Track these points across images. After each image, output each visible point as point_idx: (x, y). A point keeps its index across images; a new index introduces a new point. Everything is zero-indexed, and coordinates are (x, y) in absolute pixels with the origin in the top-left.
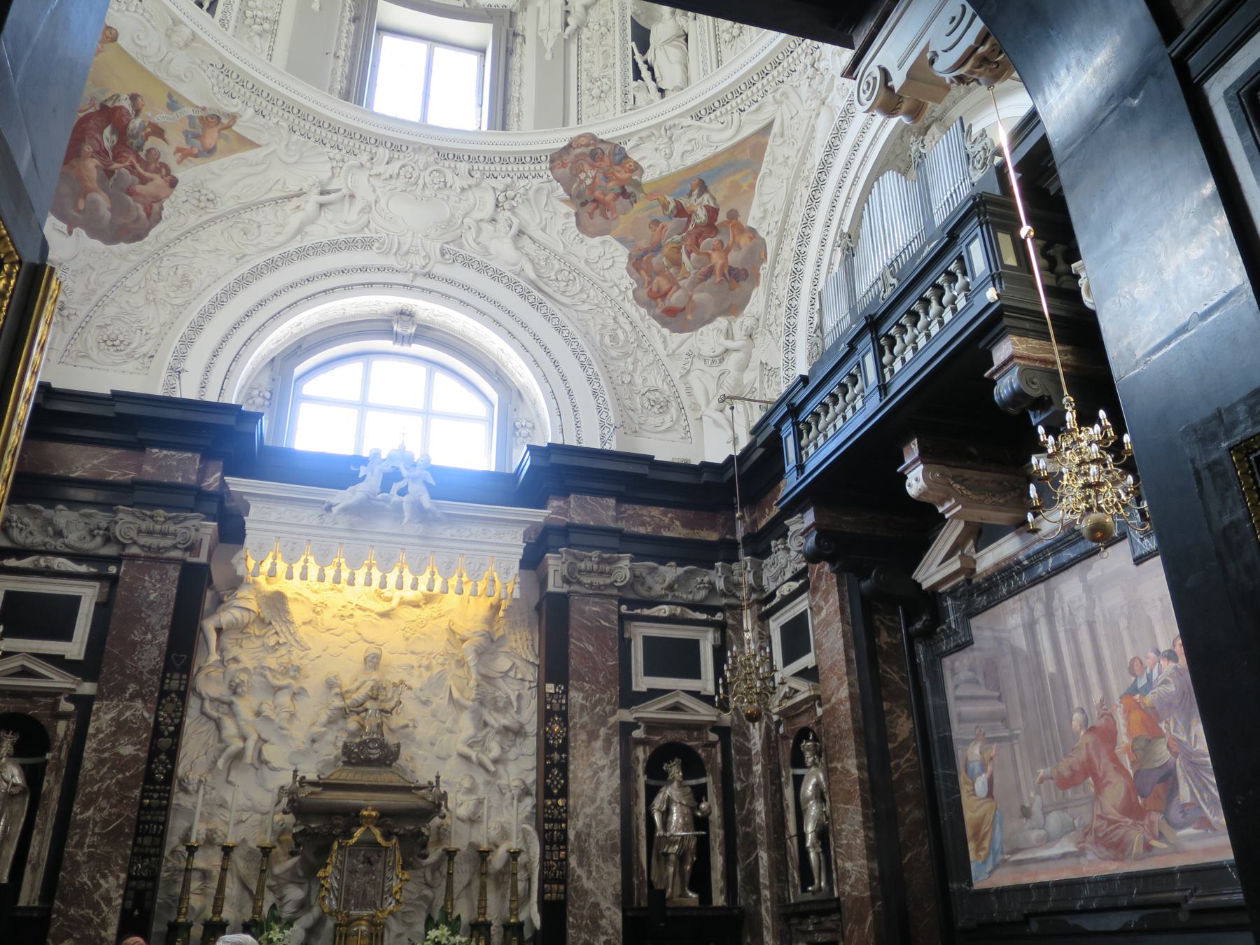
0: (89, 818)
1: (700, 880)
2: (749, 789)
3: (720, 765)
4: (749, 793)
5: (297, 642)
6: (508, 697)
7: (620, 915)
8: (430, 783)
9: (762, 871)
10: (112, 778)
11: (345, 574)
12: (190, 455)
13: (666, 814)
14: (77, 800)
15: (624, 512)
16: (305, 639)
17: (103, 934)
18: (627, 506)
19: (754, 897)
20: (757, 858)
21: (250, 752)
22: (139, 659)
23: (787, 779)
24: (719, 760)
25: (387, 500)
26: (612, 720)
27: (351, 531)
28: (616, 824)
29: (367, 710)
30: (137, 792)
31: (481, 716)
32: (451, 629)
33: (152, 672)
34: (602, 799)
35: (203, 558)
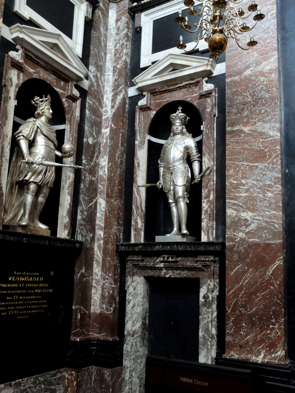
1: (49, 214)
2: (95, 147)
4: (97, 149)
9: (98, 215)
13: (32, 144)
19: (91, 235)
20: (96, 203)
23: (142, 143)
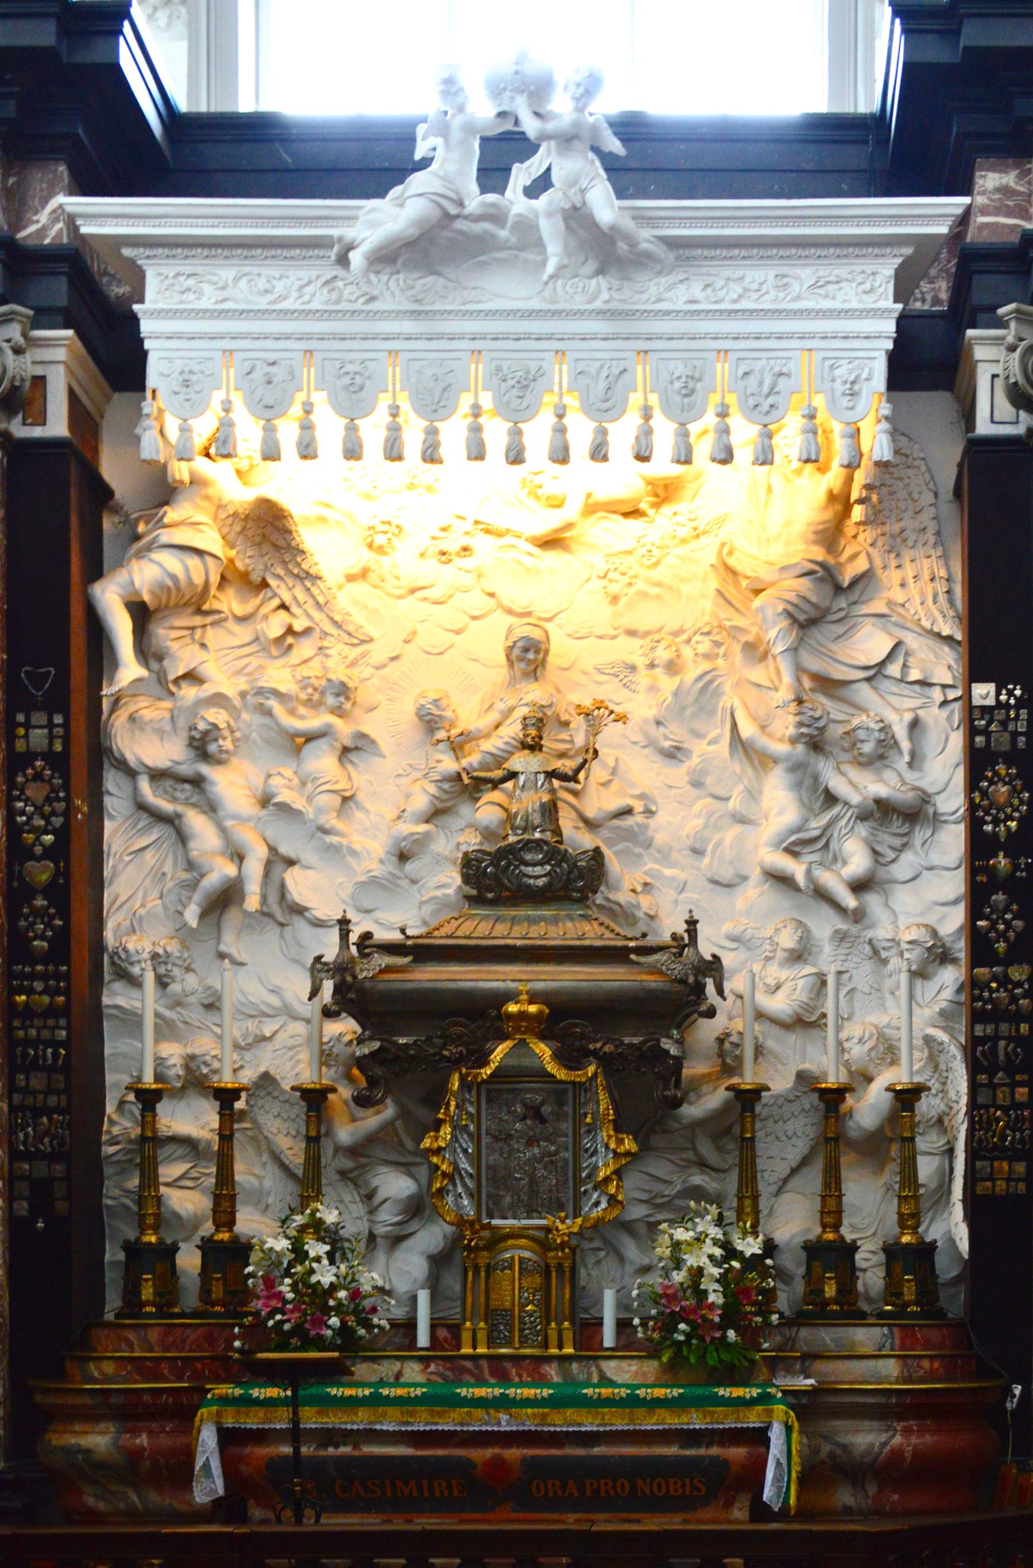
6: (885, 729)
11: (413, 440)
21: (253, 890)
25: (496, 216)
27: (416, 315)
31: (816, 778)
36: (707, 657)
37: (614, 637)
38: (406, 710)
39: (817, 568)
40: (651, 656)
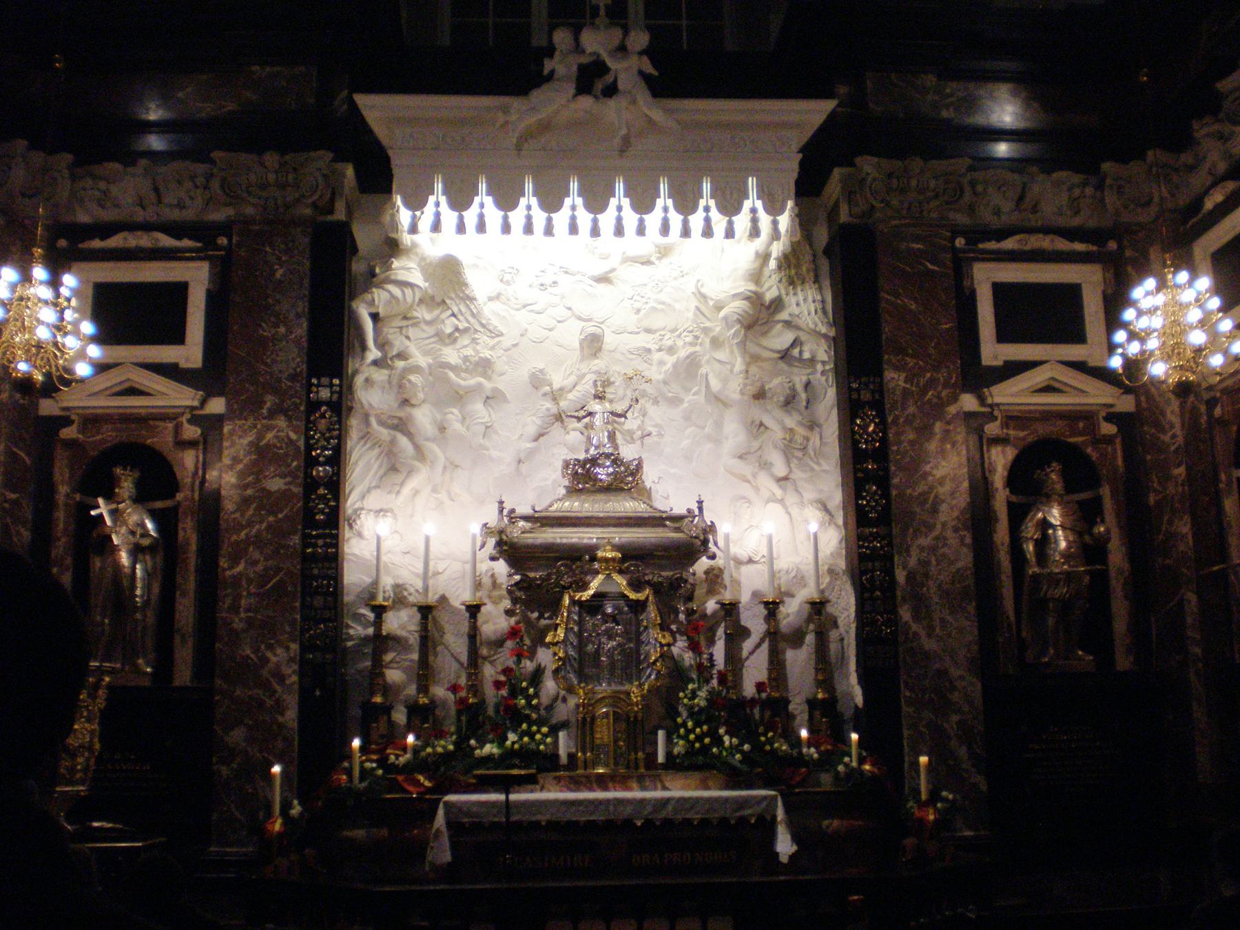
0: (240, 573)
3: (1121, 470)
5: (483, 326)
6: (793, 389)
7: (979, 686)
8: (689, 511)
9: (1189, 620)
10: (261, 522)
12: (303, 69)
14: (223, 552)
15: (952, 95)
16: (495, 322)
17: (280, 719)
18: (954, 85)
22: (274, 361)
23: (1229, 482)
24: (1120, 462)
26: (952, 409)
28: (965, 559)
29: (590, 414)
30: (296, 540)
32: (700, 293)
33: (293, 377)
34: (944, 525)
35: (340, 215)
36: (691, 344)
37: (638, 333)
38: (524, 373)
39: (753, 295)
40: (660, 343)
